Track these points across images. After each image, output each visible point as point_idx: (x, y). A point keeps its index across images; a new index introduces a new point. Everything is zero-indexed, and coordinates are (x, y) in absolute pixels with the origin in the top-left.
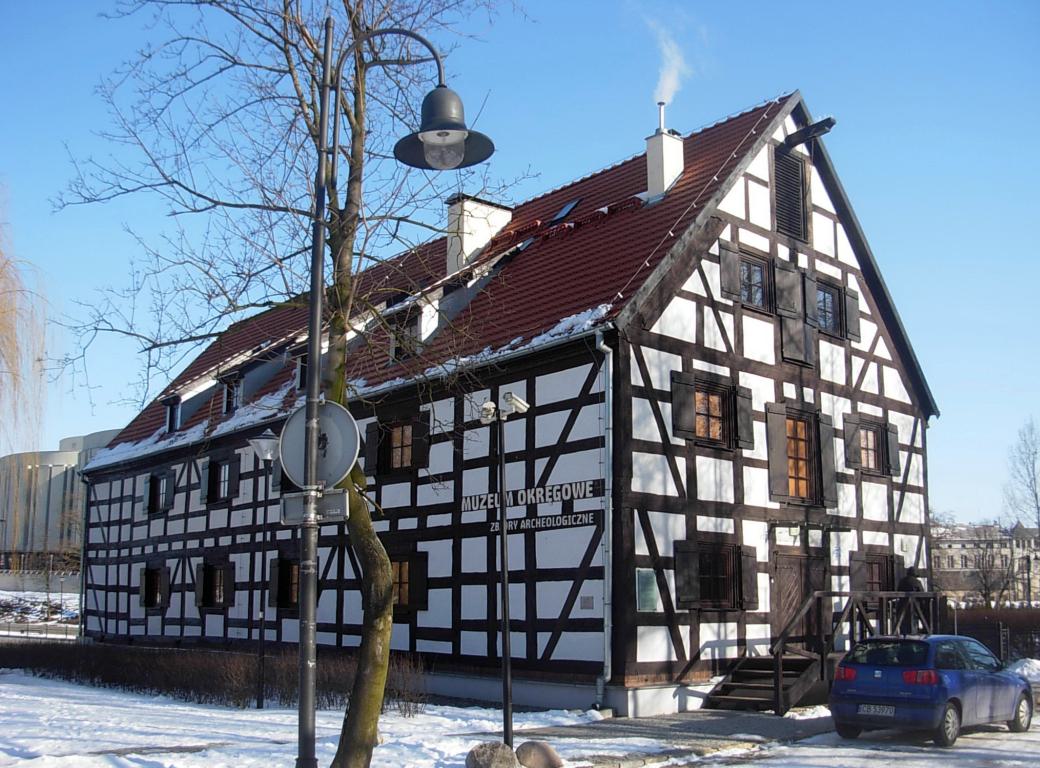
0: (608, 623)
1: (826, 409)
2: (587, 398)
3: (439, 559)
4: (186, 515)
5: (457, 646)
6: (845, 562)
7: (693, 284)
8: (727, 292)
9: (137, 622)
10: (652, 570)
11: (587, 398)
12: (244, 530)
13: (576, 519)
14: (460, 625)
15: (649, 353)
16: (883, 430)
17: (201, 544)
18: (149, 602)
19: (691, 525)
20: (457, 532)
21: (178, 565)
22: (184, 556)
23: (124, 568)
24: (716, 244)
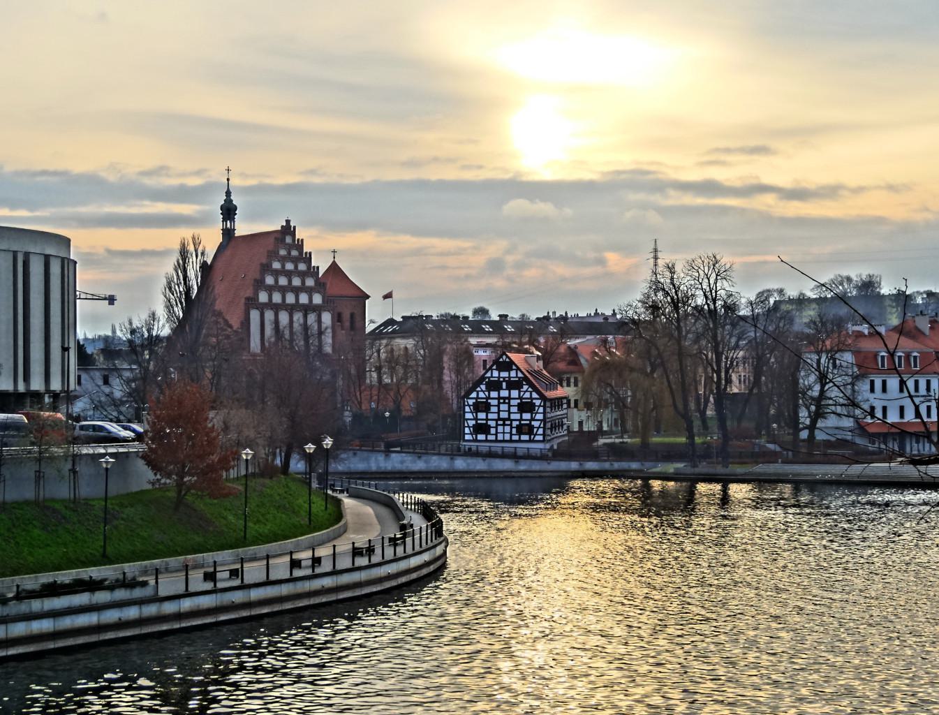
7: (479, 389)
19: (476, 422)
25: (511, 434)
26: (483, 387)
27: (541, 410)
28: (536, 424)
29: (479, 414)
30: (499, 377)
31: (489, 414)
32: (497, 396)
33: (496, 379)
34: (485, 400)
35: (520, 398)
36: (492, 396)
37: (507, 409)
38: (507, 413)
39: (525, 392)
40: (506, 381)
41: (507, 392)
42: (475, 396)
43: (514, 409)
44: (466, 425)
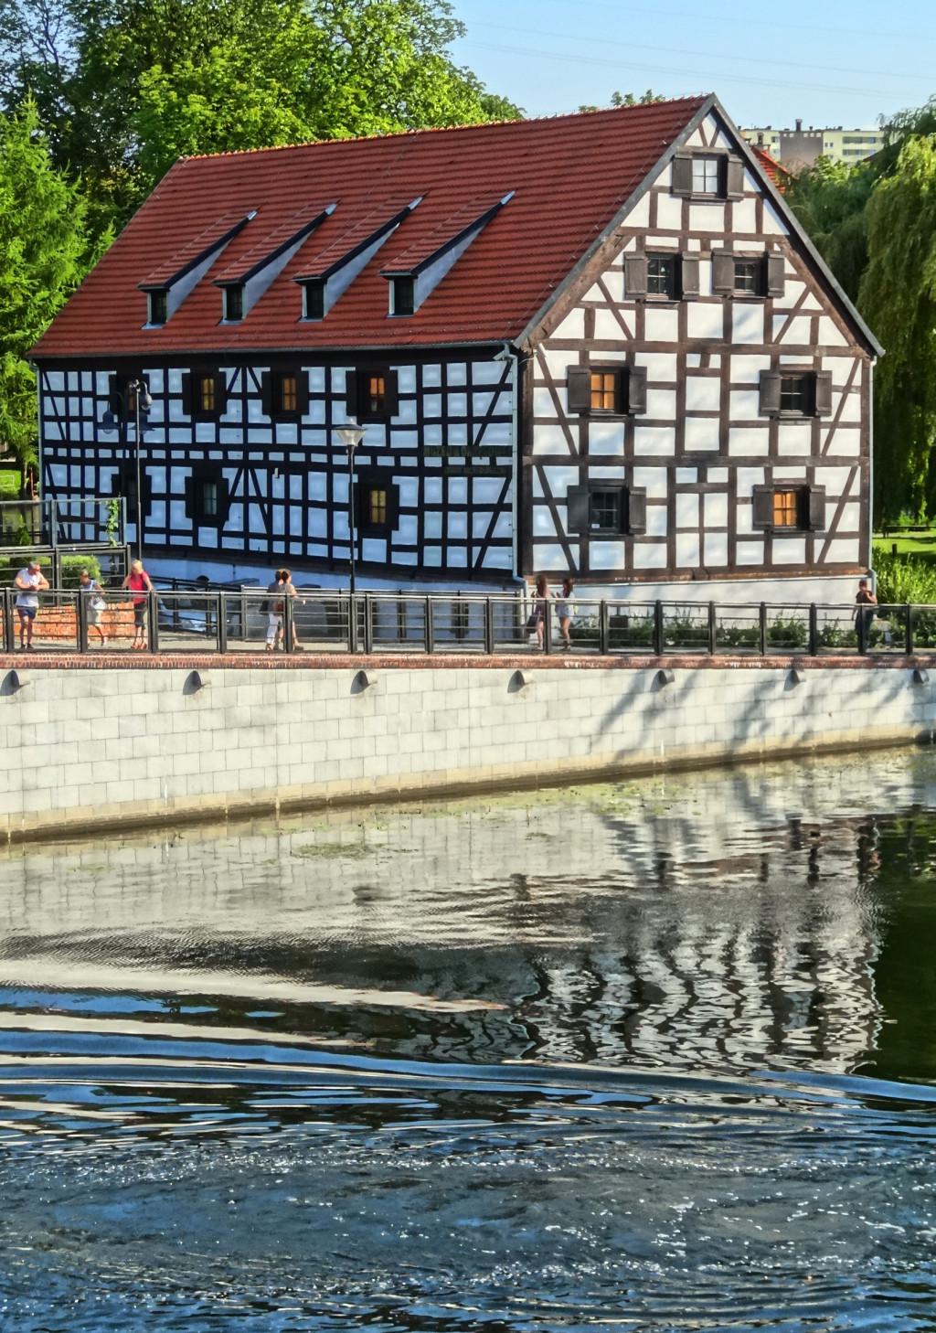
2: (503, 386)
3: (408, 490)
4: (167, 424)
7: (594, 294)
11: (503, 386)
14: (423, 542)
19: (583, 473)
20: (421, 472)
25: (733, 539)
26: (615, 282)
27: (853, 409)
28: (831, 480)
30: (685, 234)
31: (638, 430)
32: (673, 337)
33: (673, 242)
34: (621, 356)
35: (770, 346)
37: (713, 404)
38: (717, 421)
39: (791, 313)
40: (714, 256)
41: (719, 308)
42: (581, 335)
43: (745, 406)
44: (538, 492)
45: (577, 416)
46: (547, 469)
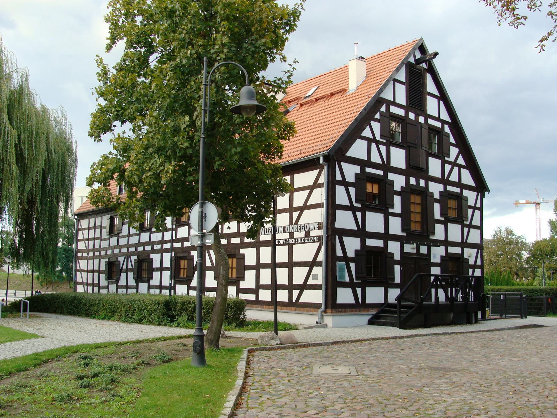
0: (323, 287)
1: (430, 190)
2: (316, 185)
5: (257, 297)
6: (438, 260)
7: (367, 133)
8: (382, 136)
9: (104, 288)
10: (344, 263)
11: (316, 185)
12: (158, 243)
13: (311, 240)
14: (259, 287)
15: (343, 164)
16: (459, 198)
17: (136, 249)
18: (109, 277)
19: (363, 243)
21: (125, 258)
22: (127, 256)
23: (96, 261)
24: (379, 113)
29: (369, 214)
31: (390, 218)
36: (393, 164)
44: (339, 253)
45: (359, 205)
46: (345, 239)
